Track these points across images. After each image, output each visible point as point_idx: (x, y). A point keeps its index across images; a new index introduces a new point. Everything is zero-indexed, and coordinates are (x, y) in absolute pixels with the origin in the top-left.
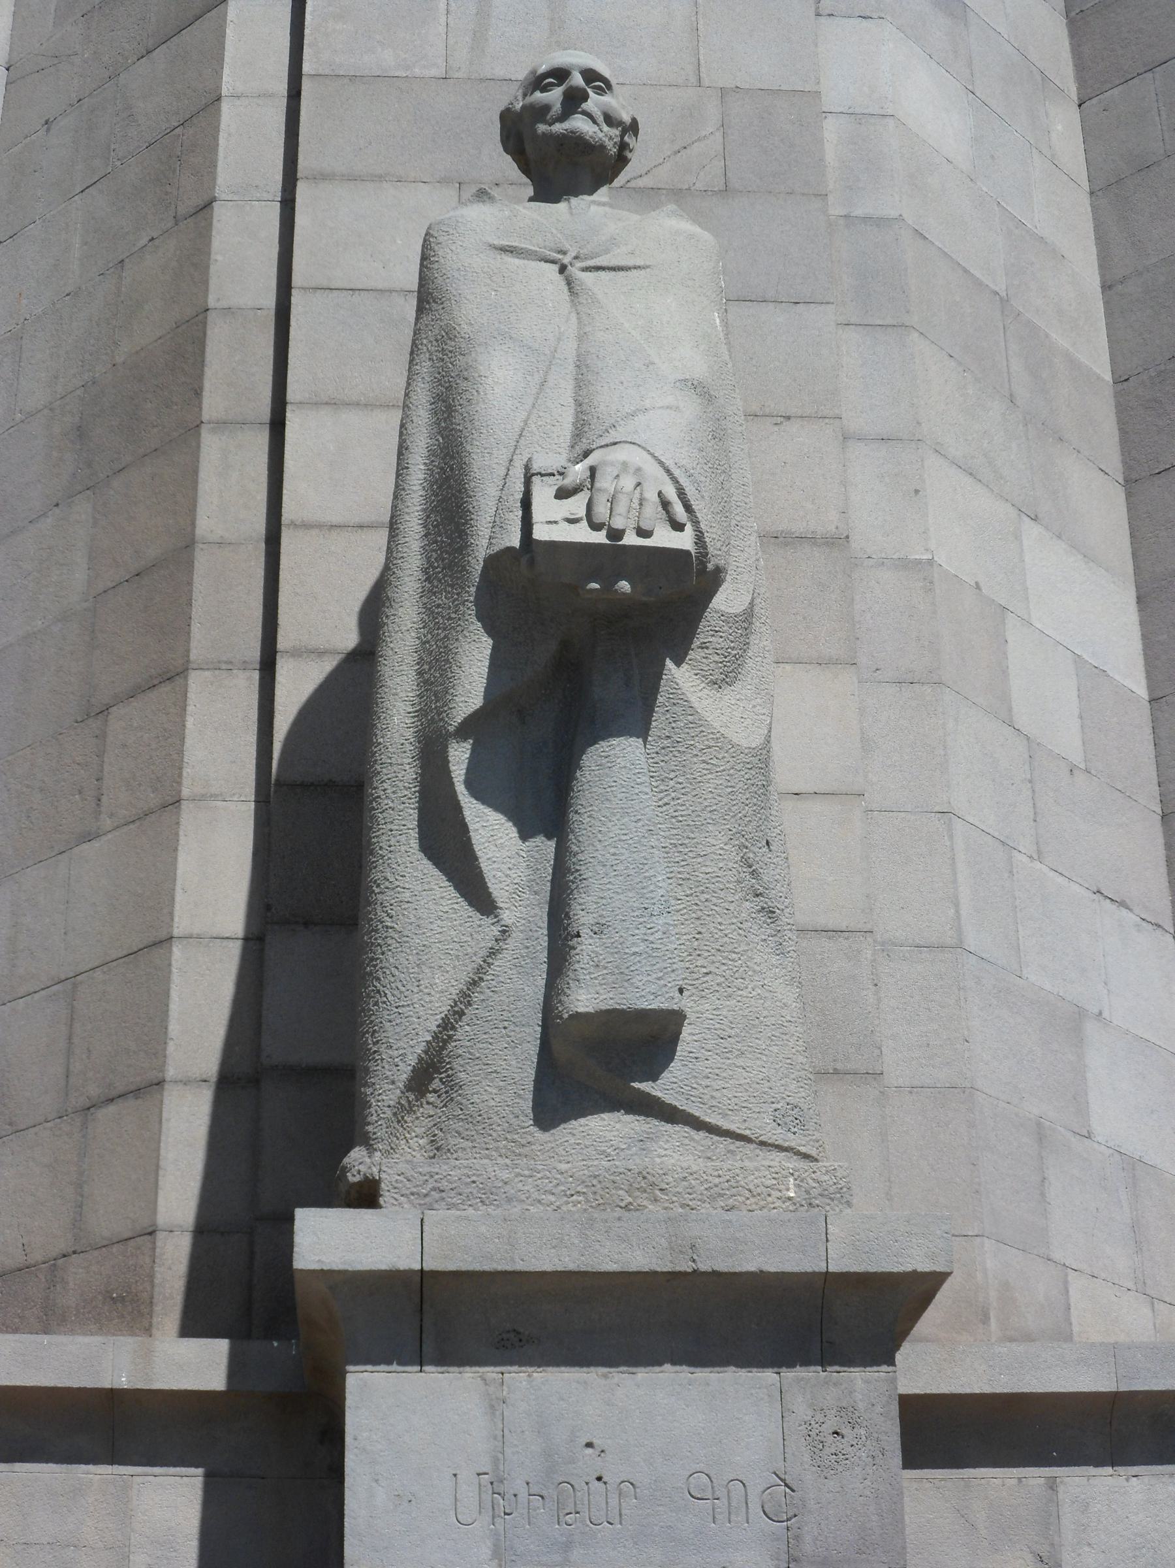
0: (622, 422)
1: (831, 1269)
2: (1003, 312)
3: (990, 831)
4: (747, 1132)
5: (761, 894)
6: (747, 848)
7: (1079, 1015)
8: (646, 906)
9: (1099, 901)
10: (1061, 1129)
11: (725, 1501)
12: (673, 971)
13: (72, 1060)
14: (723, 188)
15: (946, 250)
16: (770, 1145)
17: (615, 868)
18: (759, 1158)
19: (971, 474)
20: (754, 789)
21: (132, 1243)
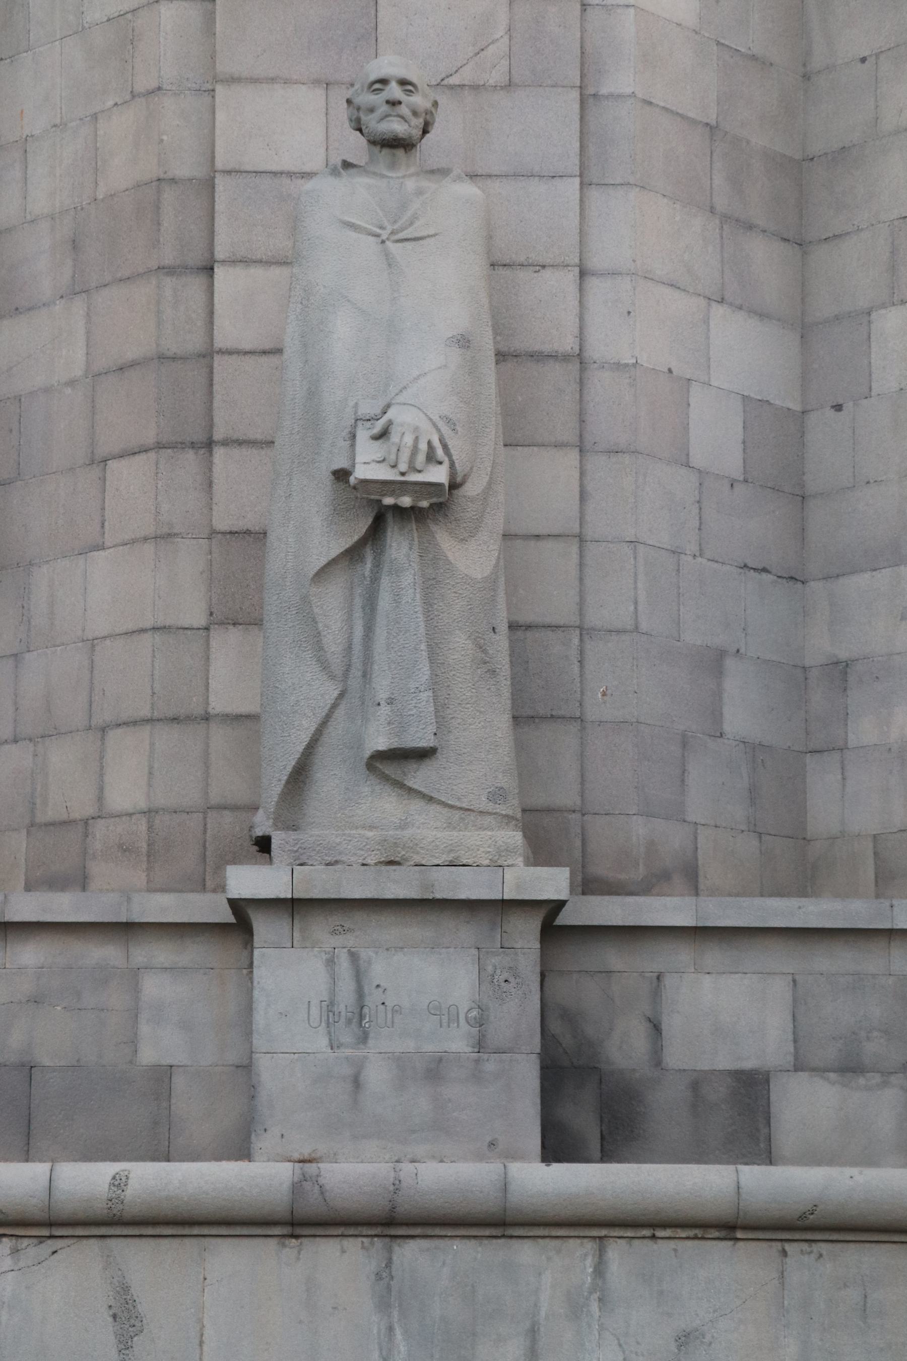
0: (410, 385)
1: (505, 898)
2: (712, 139)
3: (665, 546)
4: (472, 807)
5: (488, 662)
6: (479, 637)
7: (721, 654)
8: (417, 686)
9: (745, 573)
10: (701, 736)
11: (447, 1015)
12: (431, 724)
13: (93, 695)
14: (507, 83)
15: (668, 106)
16: (484, 813)
17: (400, 664)
18: (478, 820)
19: (672, 285)
20: (486, 601)
21: (134, 817)
